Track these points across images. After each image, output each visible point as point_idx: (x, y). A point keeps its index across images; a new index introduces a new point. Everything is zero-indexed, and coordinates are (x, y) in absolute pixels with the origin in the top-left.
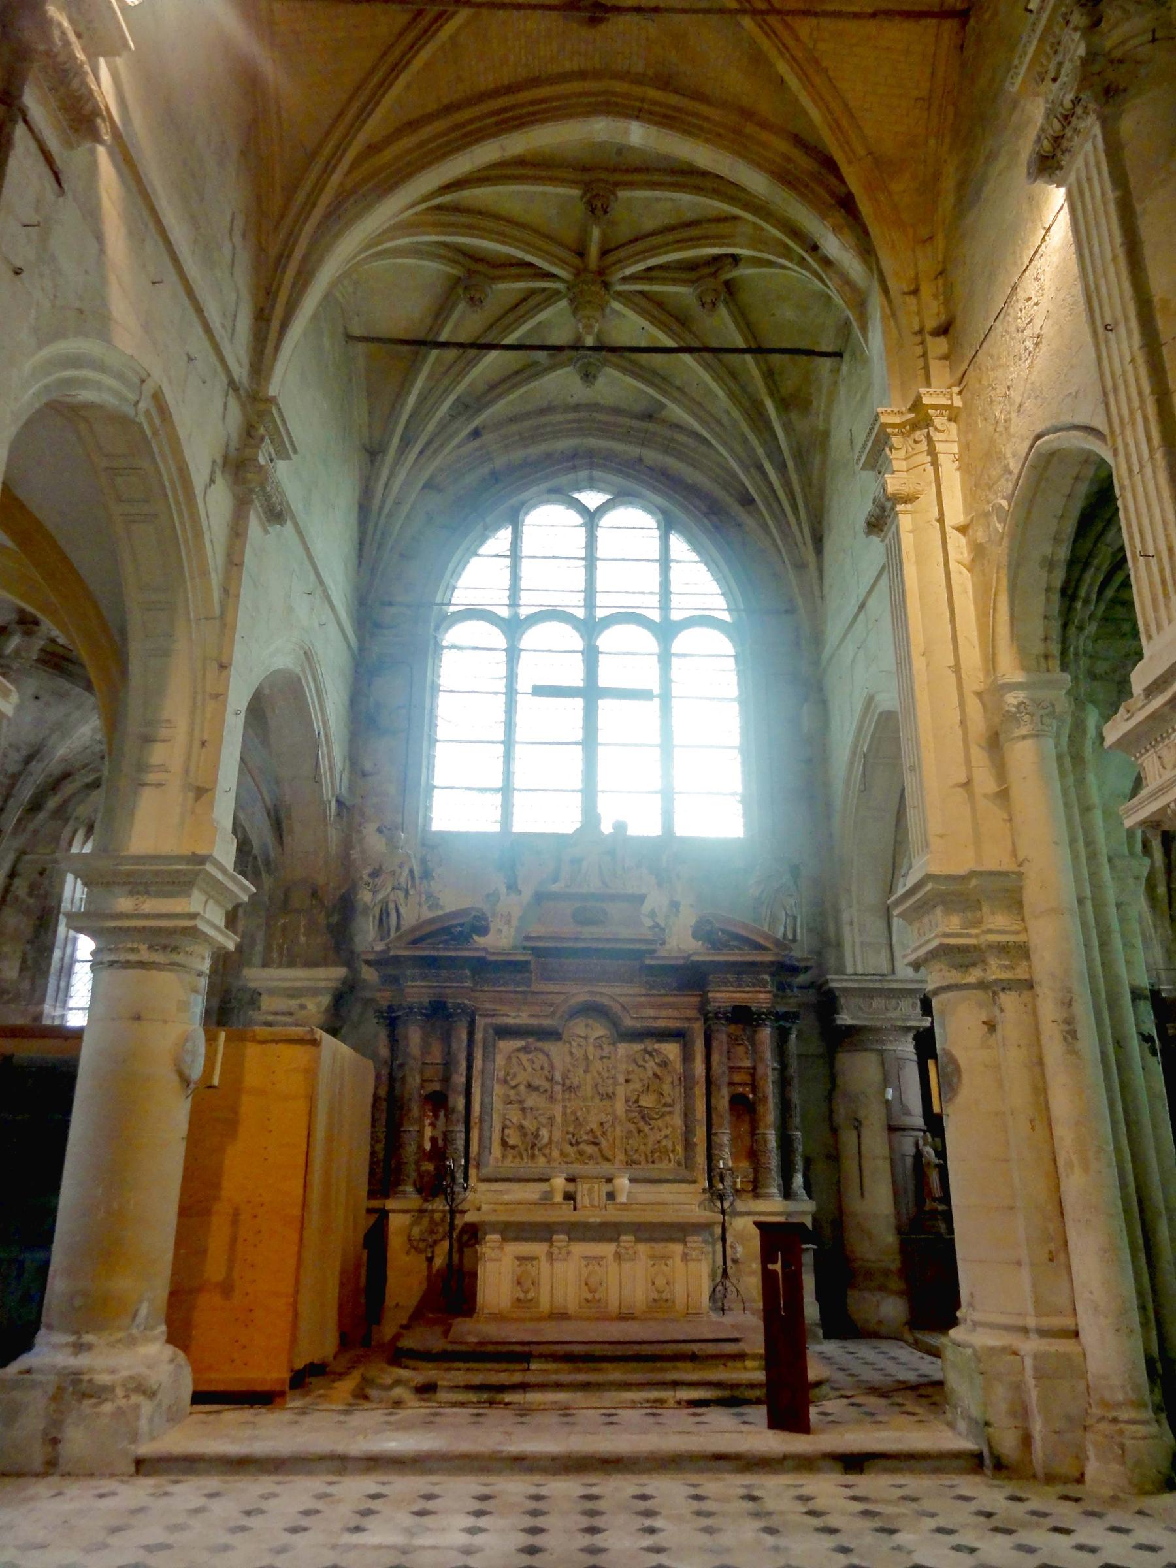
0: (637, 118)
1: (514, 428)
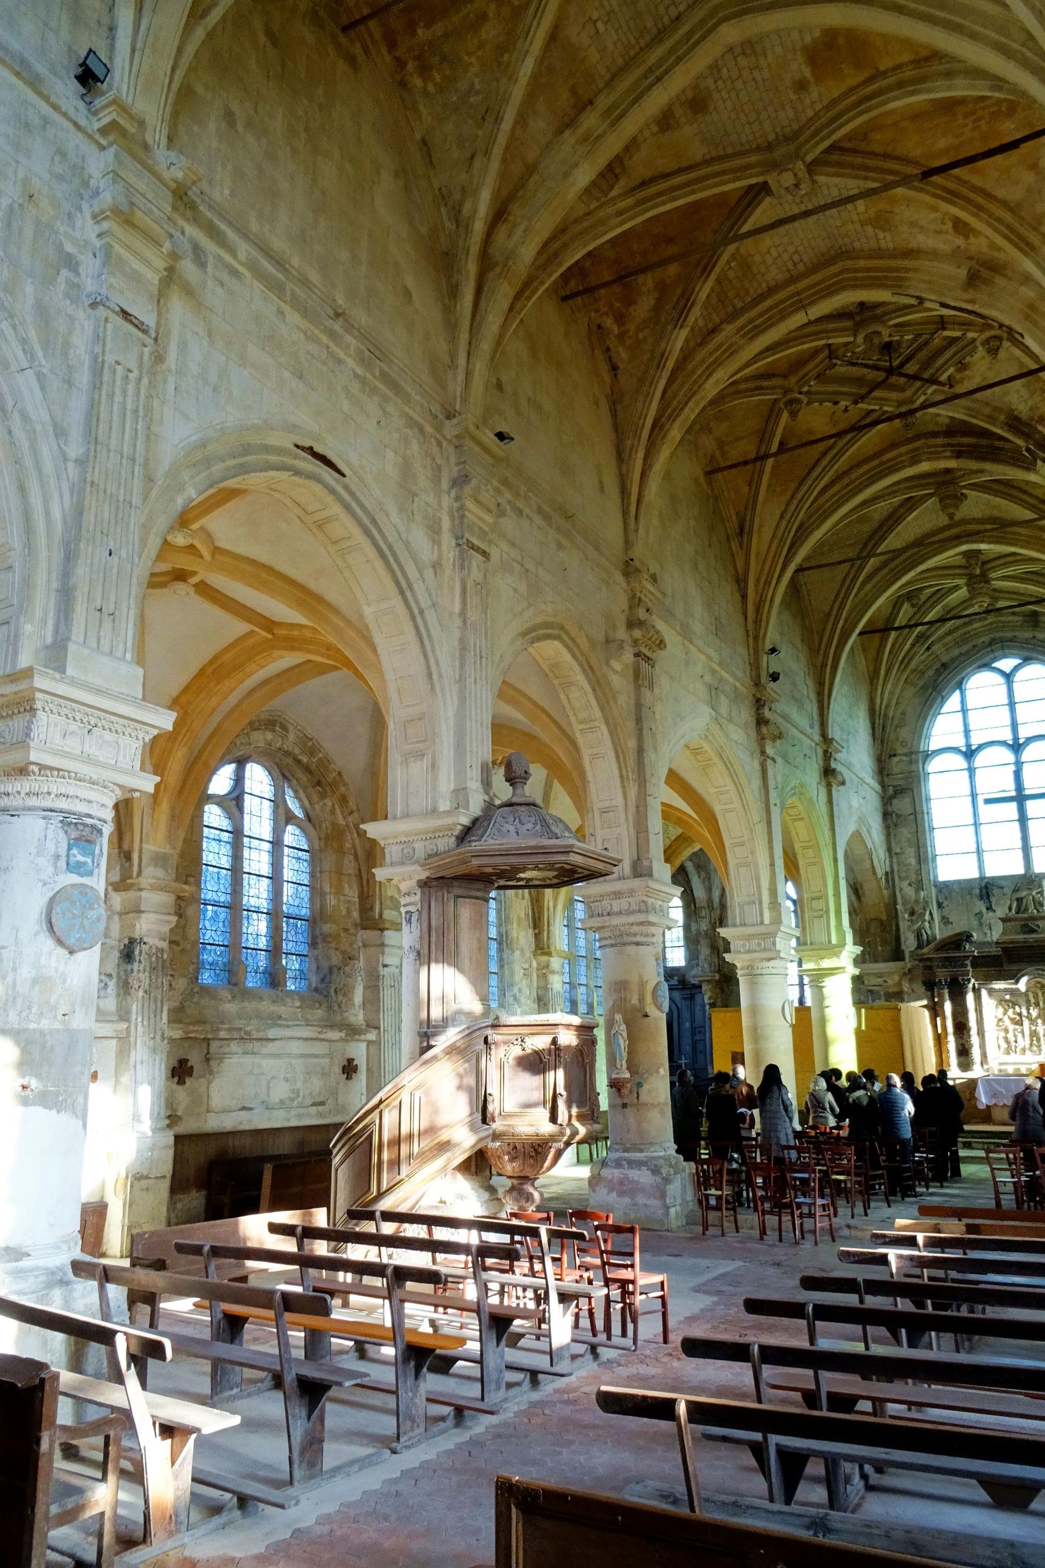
0: (982, 542)
1: (949, 638)
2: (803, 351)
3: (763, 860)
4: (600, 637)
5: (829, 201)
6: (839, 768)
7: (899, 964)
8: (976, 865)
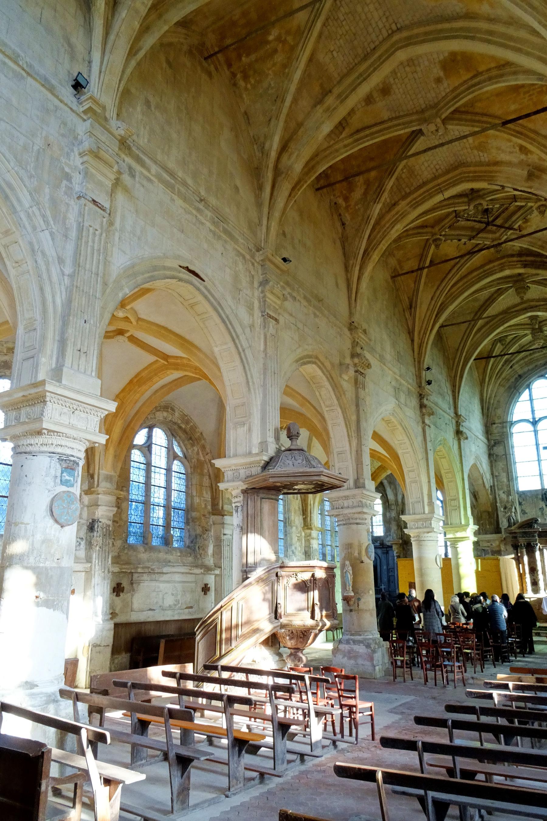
0: (539, 311)
1: (522, 362)
2: (442, 214)
3: (424, 479)
4: (337, 362)
5: (454, 137)
6: (464, 430)
7: (499, 535)
8: (540, 482)
